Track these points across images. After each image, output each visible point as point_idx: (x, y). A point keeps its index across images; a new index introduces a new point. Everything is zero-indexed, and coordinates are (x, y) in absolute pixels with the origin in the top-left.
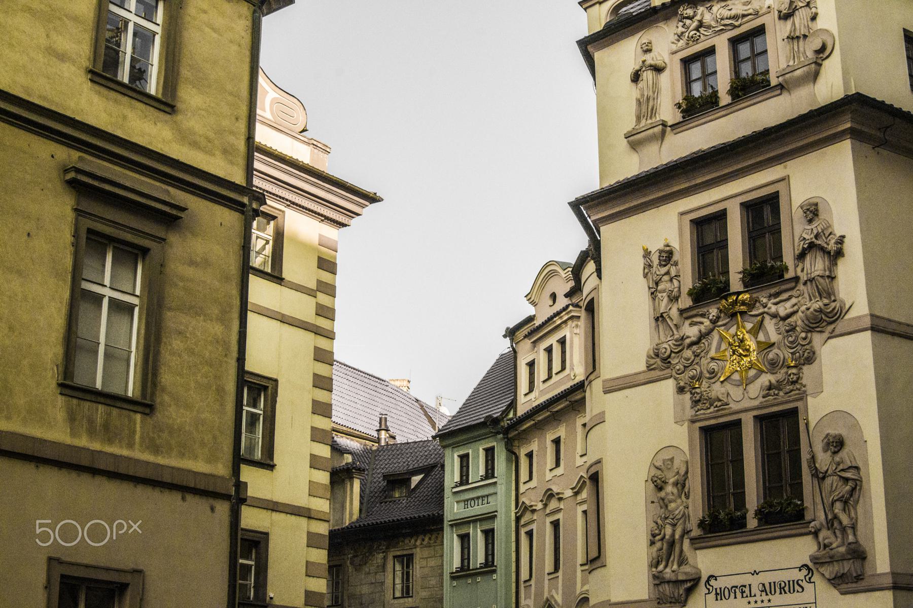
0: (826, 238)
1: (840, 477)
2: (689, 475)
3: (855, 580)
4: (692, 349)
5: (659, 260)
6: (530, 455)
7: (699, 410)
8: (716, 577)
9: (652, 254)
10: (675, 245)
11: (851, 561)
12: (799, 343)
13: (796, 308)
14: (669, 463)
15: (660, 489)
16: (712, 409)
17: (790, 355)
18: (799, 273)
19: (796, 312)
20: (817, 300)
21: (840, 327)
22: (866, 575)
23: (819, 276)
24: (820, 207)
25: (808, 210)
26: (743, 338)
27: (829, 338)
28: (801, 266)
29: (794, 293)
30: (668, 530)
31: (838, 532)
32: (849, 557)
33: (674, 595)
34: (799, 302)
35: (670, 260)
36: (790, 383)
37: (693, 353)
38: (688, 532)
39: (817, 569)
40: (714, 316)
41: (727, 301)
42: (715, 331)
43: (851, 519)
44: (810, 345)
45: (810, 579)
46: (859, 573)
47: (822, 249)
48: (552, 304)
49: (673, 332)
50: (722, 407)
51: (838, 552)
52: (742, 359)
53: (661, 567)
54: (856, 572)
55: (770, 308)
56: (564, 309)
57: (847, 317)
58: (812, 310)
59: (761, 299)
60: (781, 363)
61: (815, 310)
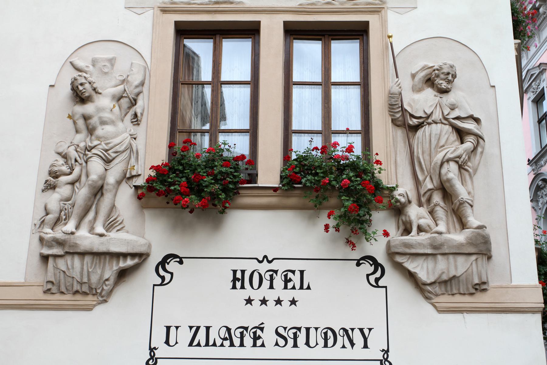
2: (145, 89)
3: (474, 291)
8: (181, 258)
11: (474, 258)
14: (108, 64)
22: (491, 284)
31: (440, 212)
32: (472, 250)
33: (89, 279)
38: (132, 177)
39: (399, 267)
43: (469, 193)
45: (377, 280)
46: (484, 279)
51: (448, 241)
53: (70, 226)
54: (480, 277)
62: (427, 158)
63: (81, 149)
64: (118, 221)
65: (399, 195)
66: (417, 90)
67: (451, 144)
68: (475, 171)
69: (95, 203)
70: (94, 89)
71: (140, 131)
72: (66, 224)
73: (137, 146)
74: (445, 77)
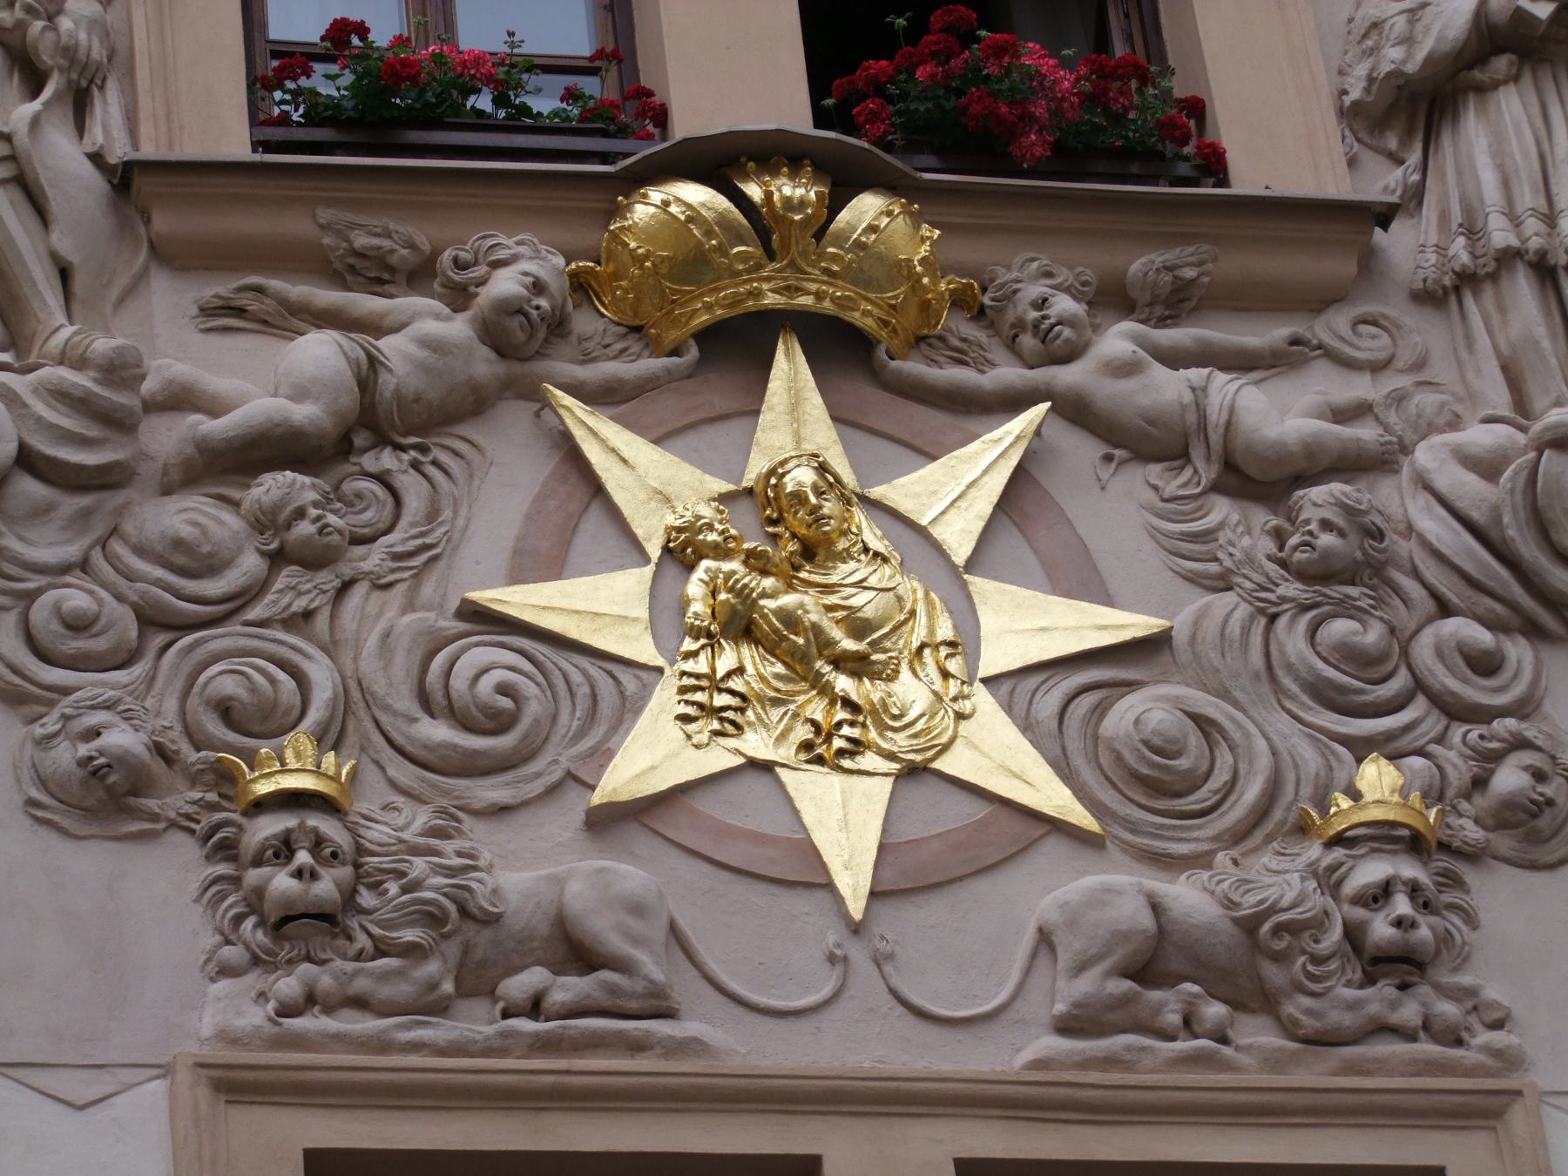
7: (311, 1000)
12: (1420, 685)
13: (1366, 433)
29: (1333, 326)
34: (1399, 399)
37: (265, 522)
40: (538, 287)
42: (514, 417)
60: (1251, 792)
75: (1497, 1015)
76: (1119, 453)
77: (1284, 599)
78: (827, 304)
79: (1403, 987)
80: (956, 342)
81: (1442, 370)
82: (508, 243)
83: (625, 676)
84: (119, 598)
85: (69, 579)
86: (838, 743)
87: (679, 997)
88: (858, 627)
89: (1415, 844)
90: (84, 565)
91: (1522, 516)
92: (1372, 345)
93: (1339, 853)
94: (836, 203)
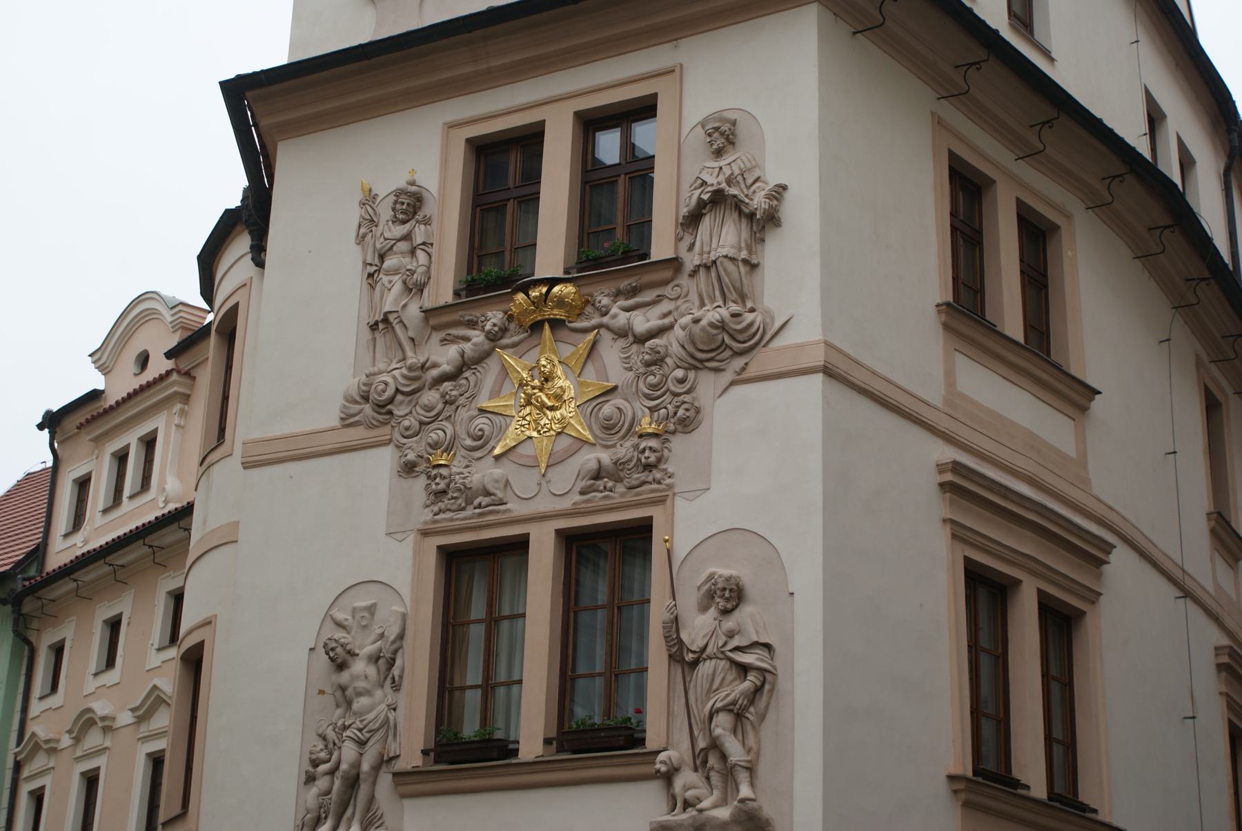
0: (748, 188)
1: (733, 662)
4: (442, 389)
5: (394, 210)
6: (58, 650)
7: (440, 511)
9: (379, 199)
10: (430, 182)
13: (667, 321)
14: (366, 614)
15: (341, 666)
16: (469, 512)
17: (647, 411)
18: (683, 254)
19: (670, 327)
20: (716, 304)
21: (760, 362)
23: (726, 257)
24: (741, 130)
25: (716, 129)
26: (551, 372)
27: (733, 383)
28: (688, 240)
29: (668, 291)
30: (349, 752)
31: (715, 778)
34: (677, 308)
35: (415, 213)
36: (641, 469)
37: (443, 396)
38: (391, 759)
40: (495, 325)
41: (527, 295)
43: (749, 751)
44: (693, 394)
47: (737, 205)
48: (137, 372)
49: (403, 351)
50: (490, 508)
52: (545, 414)
55: (615, 316)
56: (162, 378)
57: (777, 343)
58: (704, 322)
59: (598, 298)
61: (712, 325)
62: (700, 707)
63: (339, 730)
64: (376, 817)
65: (661, 762)
66: (704, 609)
67: (729, 685)
68: (762, 717)
69: (354, 795)
70: (349, 652)
71: (402, 699)
72: (325, 823)
73: (395, 719)
74: (722, 594)
75: (669, 475)
76: (615, 337)
77: (640, 373)
78: (552, 316)
79: (651, 471)
80: (587, 313)
81: (690, 297)
82: (490, 314)
83: (507, 419)
84: (416, 420)
85: (407, 417)
86: (545, 430)
87: (505, 501)
88: (558, 397)
89: (655, 435)
90: (411, 412)
91: (689, 342)
92: (674, 294)
93: (640, 440)
94: (549, 291)
